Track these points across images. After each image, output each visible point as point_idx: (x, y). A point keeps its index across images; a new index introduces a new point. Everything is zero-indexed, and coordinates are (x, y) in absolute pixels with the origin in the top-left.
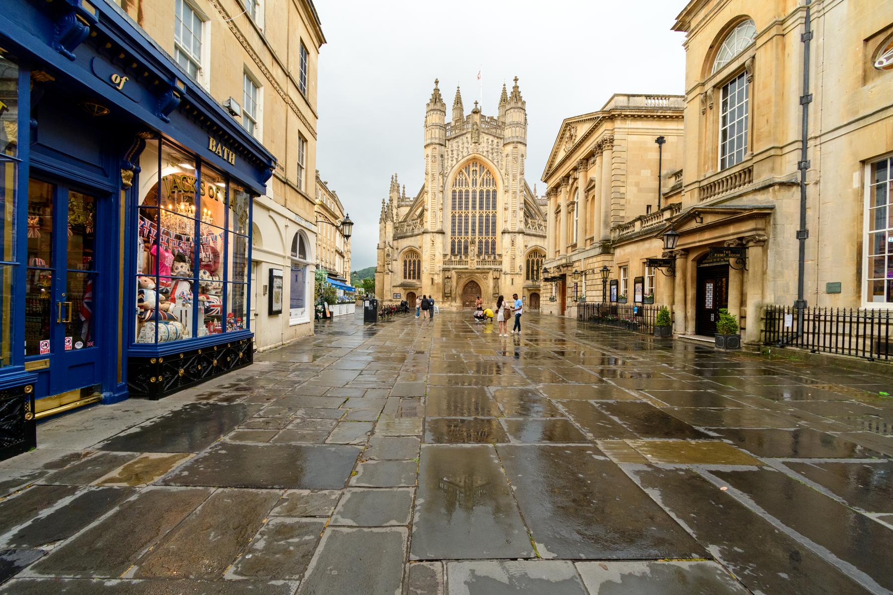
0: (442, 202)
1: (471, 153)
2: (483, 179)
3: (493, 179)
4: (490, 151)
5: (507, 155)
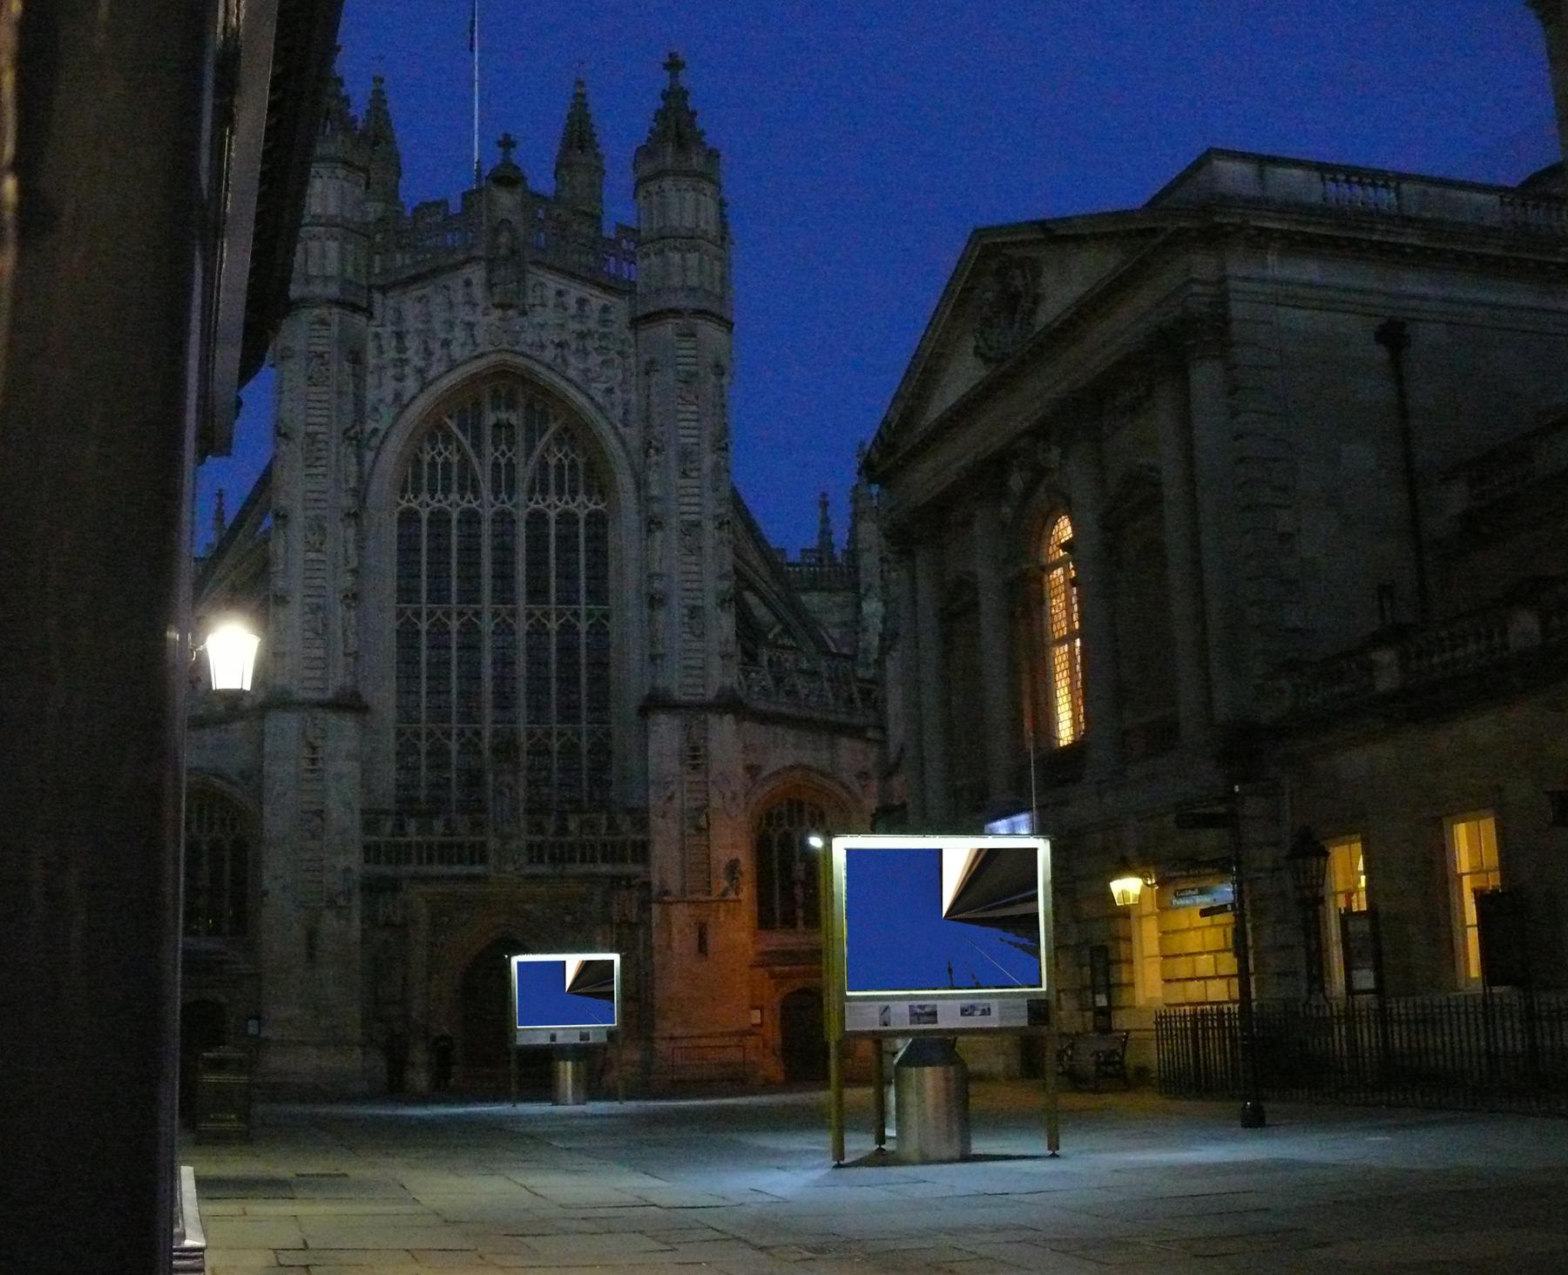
0: (354, 564)
2: (544, 466)
3: (590, 466)
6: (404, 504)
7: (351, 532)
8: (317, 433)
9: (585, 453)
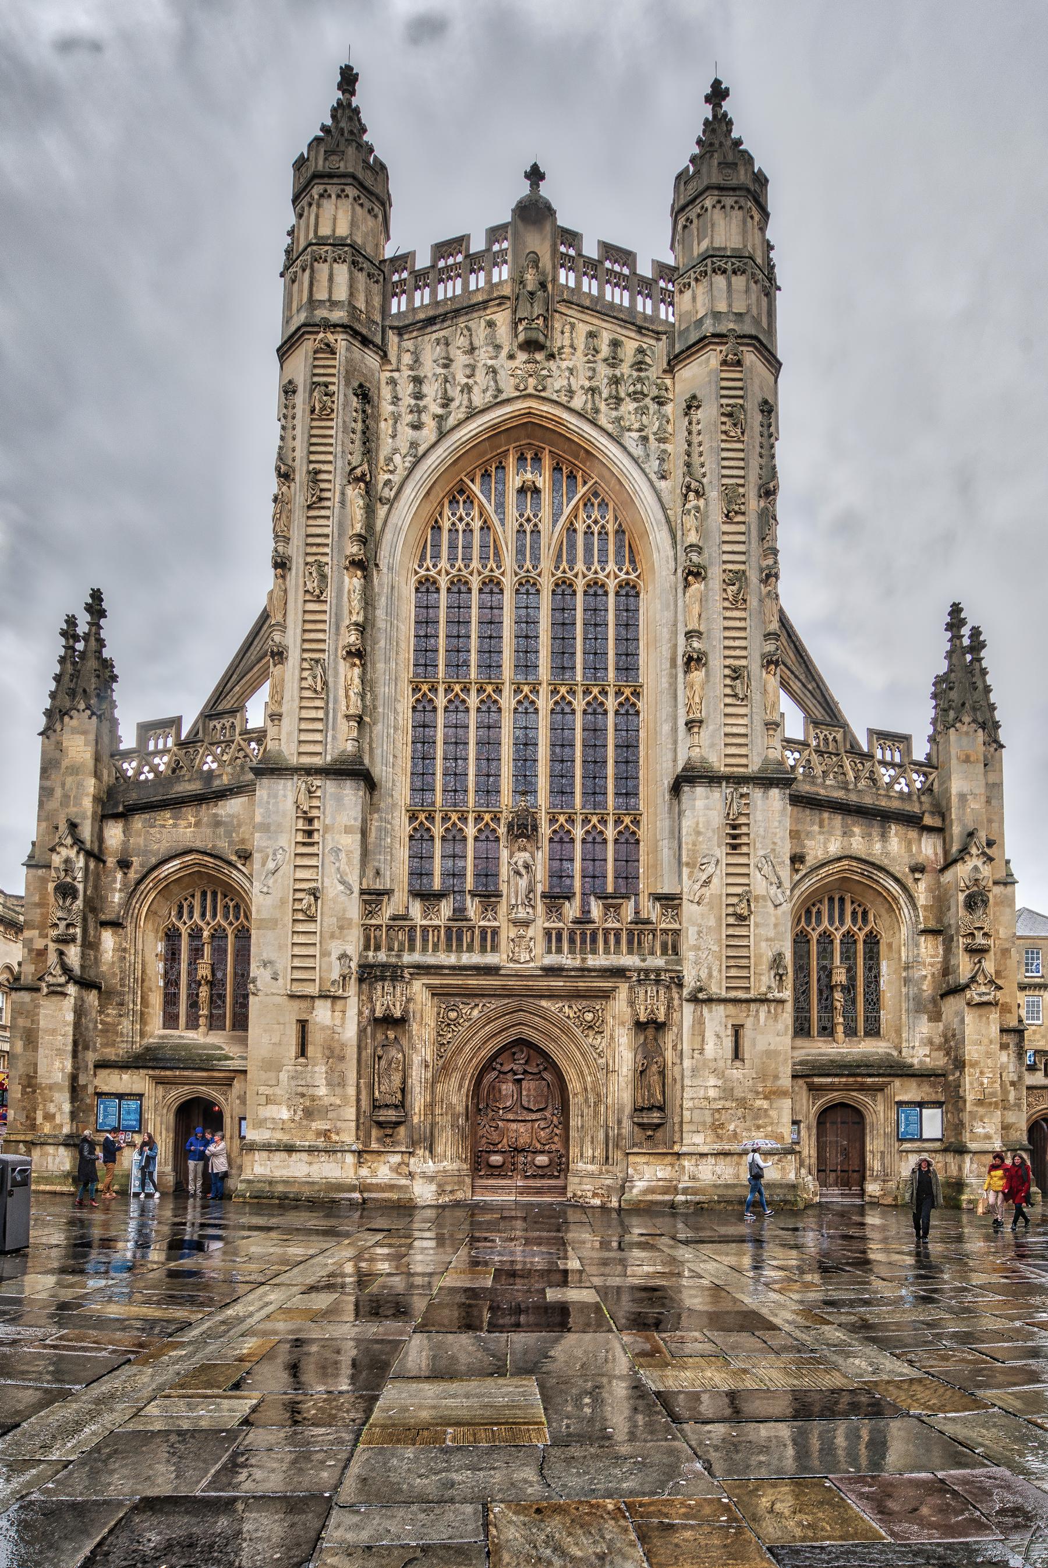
1: (509, 392)
5: (692, 404)
8: (320, 472)
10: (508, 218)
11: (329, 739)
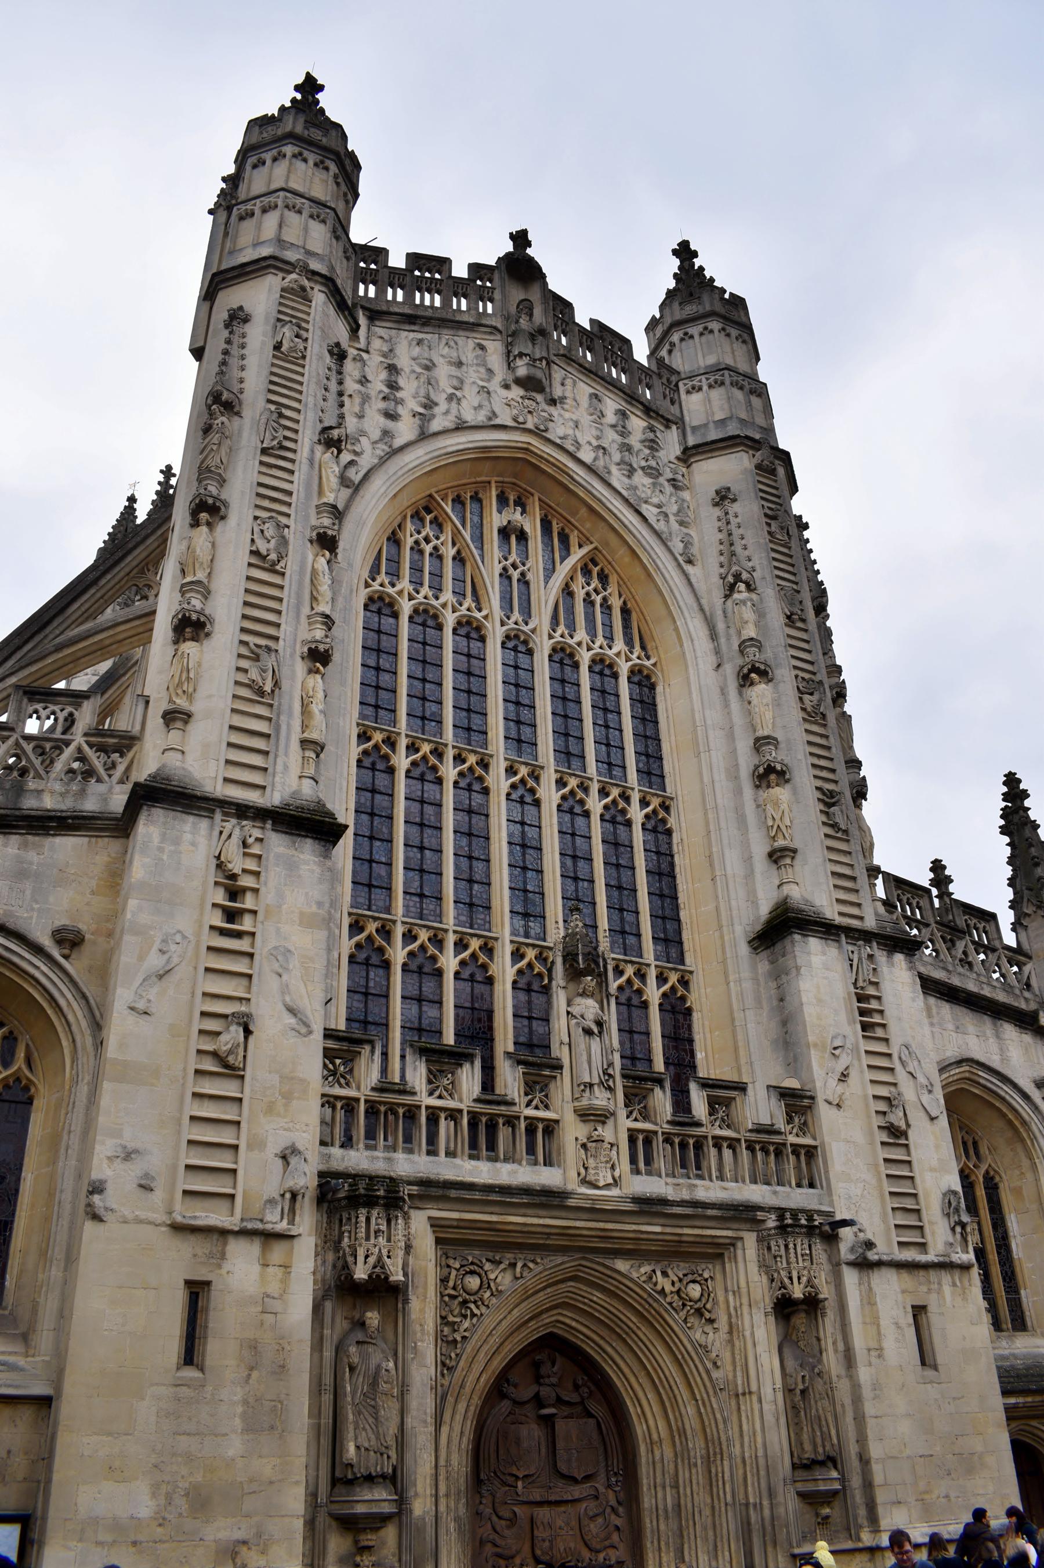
1: (505, 418)
3: (625, 611)
4: (617, 457)
6: (376, 586)
7: (322, 563)
9: (620, 596)
10: (492, 262)
11: (279, 767)
